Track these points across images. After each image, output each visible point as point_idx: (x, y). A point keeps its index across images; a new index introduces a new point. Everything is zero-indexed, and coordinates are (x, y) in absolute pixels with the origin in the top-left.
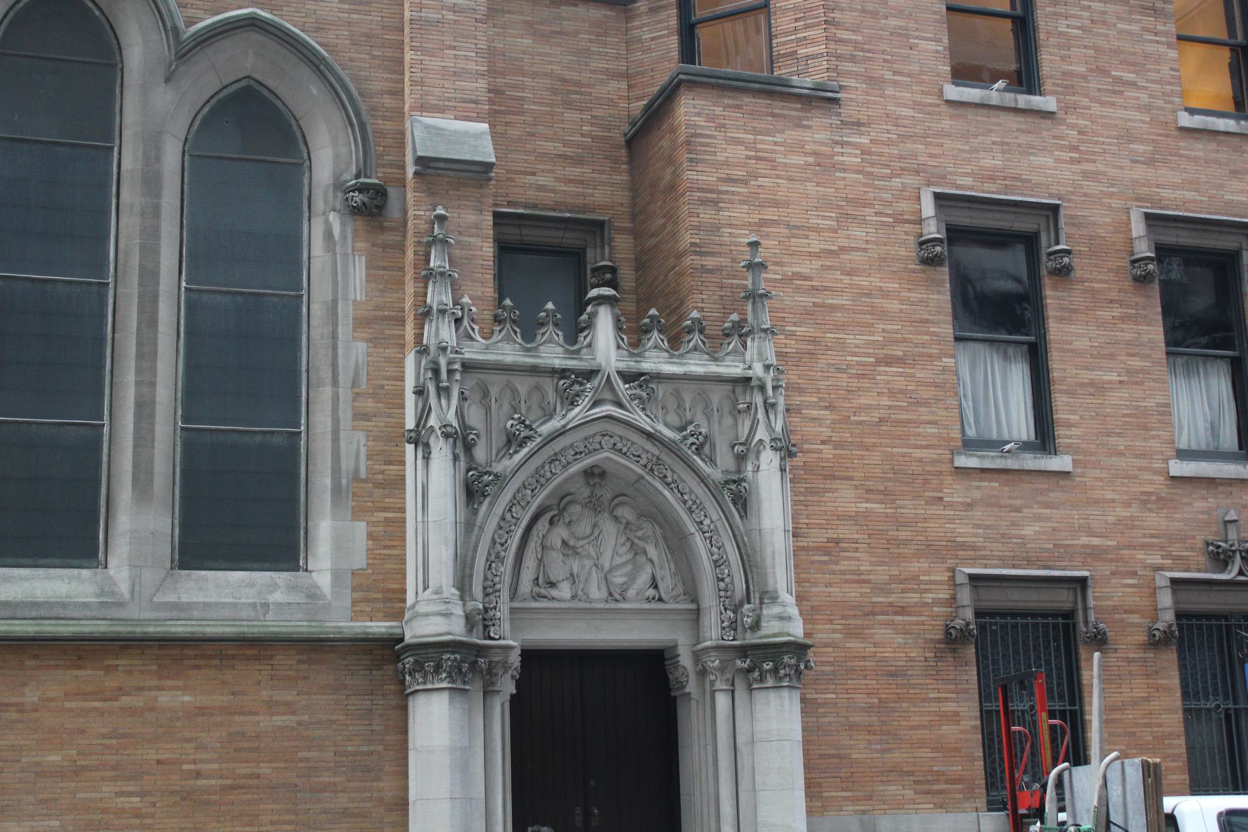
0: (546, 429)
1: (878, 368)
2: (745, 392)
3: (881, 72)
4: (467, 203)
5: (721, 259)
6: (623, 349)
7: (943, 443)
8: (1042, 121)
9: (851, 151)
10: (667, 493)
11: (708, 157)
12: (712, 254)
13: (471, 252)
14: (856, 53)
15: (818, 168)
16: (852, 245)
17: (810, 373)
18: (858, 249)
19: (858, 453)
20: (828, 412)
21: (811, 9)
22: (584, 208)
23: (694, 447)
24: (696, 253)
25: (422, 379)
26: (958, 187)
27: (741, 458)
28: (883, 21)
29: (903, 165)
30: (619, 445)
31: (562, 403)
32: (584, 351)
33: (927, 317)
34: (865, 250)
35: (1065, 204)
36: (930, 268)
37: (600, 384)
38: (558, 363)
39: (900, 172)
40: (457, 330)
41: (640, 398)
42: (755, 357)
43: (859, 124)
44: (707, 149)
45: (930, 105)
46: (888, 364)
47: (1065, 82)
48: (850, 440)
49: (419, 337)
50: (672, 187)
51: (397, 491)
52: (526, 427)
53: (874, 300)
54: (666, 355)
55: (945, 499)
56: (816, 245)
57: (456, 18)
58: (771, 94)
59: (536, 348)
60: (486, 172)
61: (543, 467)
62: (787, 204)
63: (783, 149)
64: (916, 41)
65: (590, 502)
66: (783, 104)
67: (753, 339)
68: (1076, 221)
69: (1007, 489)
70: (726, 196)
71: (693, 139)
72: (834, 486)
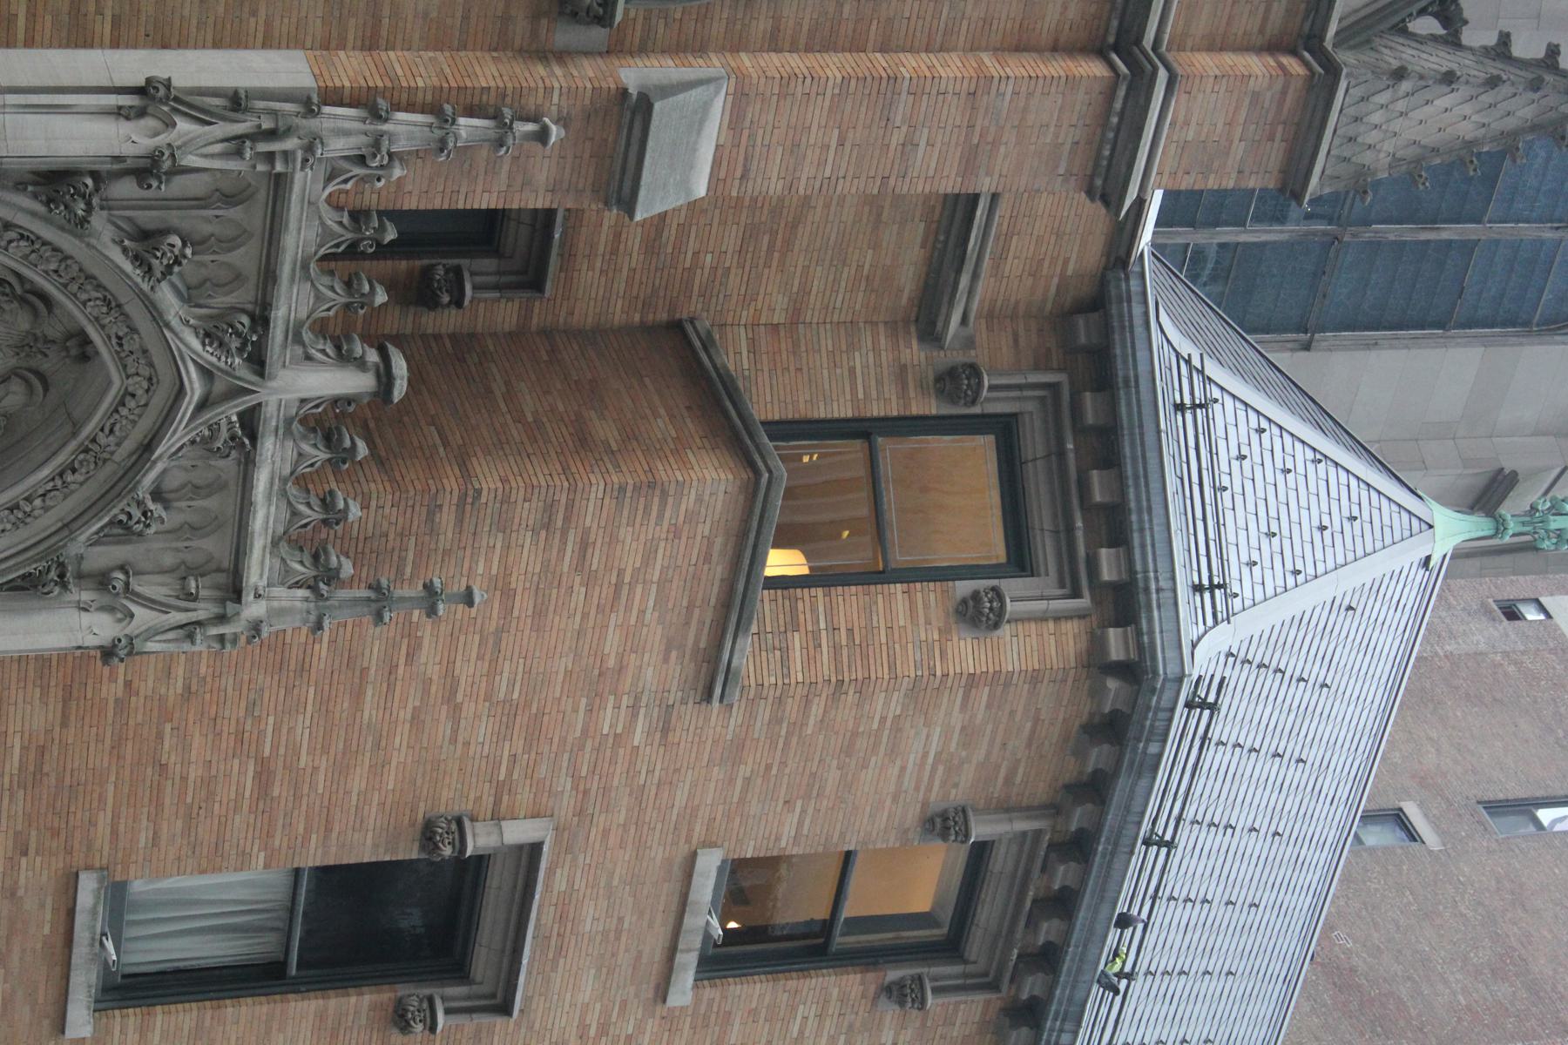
0: (167, 297)
1: (252, 762)
2: (218, 587)
3: (750, 761)
4: (568, 170)
5: (450, 535)
6: (300, 408)
7: (120, 855)
8: (652, 985)
9: (621, 719)
10: (45, 472)
11: (626, 513)
12: (460, 521)
13: (481, 178)
14: (785, 725)
15: (596, 672)
16: (463, 722)
17: (248, 664)
18: (455, 731)
19: (109, 734)
20: (179, 691)
21: (865, 657)
22: (568, 256)
23: (124, 518)
24: (463, 498)
25: (261, 104)
26: (551, 872)
27: (102, 581)
28: (835, 762)
29: (593, 793)
30: (131, 403)
31: (211, 317)
32: (299, 350)
33: (336, 828)
34: (454, 741)
35: (511, 1025)
36: (418, 836)
37: (239, 379)
38: (279, 314)
39: (581, 788)
40: (346, 158)
41: (212, 438)
42: (275, 604)
43: (666, 731)
44: (640, 512)
45: (690, 830)
46: (258, 775)
47: (713, 1017)
48: (131, 722)
49: (334, 97)
50: (583, 441)
51: (64, 34)
52: (169, 268)
53: (368, 755)
54: (287, 471)
55: (24, 861)
56: (467, 670)
57: (892, 147)
58: (726, 605)
59: (307, 277)
60: (619, 201)
61: (99, 286)
62: (538, 629)
63: (633, 622)
64: (798, 809)
65: (36, 339)
66: (708, 622)
67: (306, 600)
68: (484, 1034)
69: (39, 946)
70: (557, 541)
71: (658, 492)
72: (52, 700)
